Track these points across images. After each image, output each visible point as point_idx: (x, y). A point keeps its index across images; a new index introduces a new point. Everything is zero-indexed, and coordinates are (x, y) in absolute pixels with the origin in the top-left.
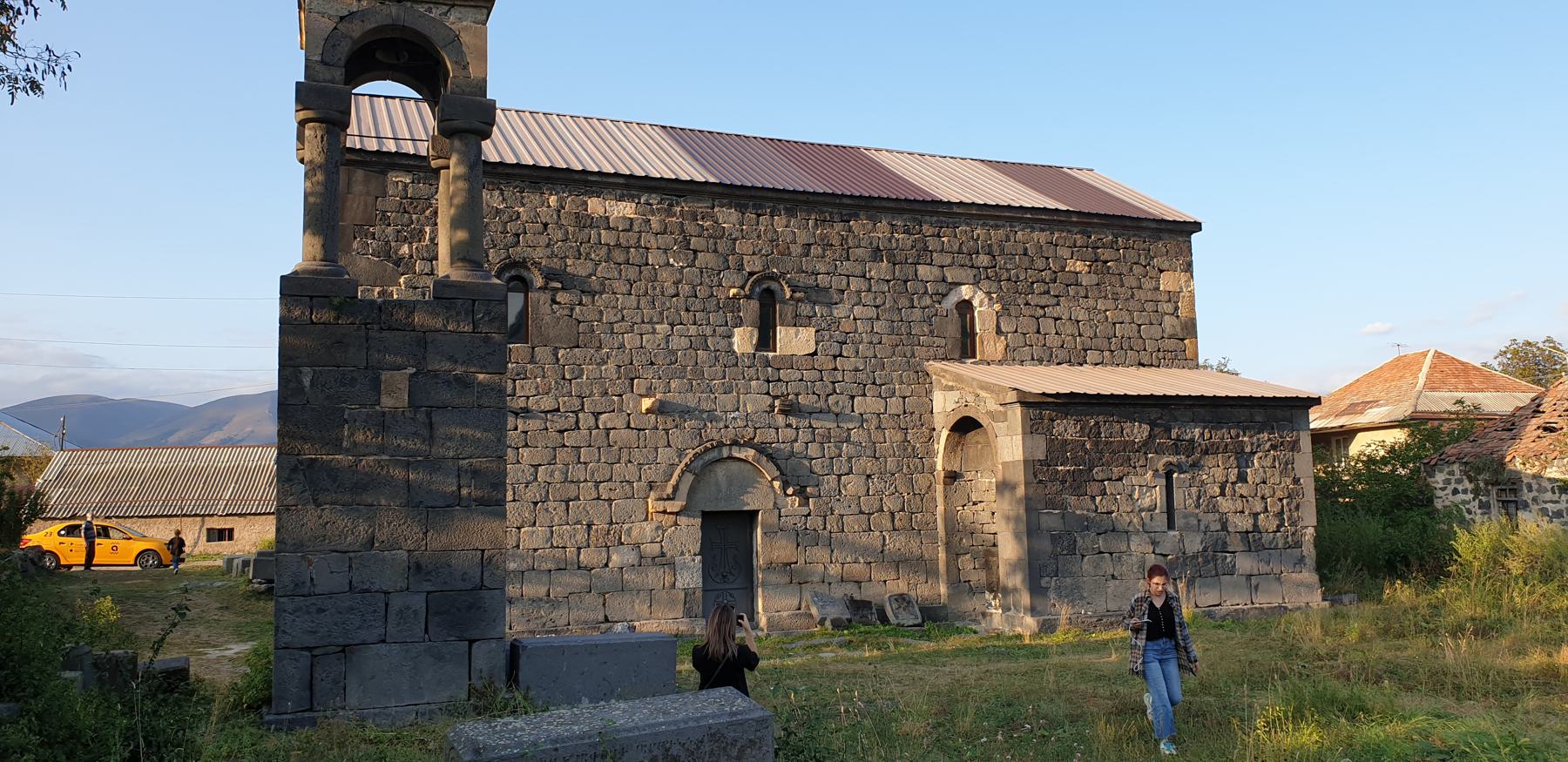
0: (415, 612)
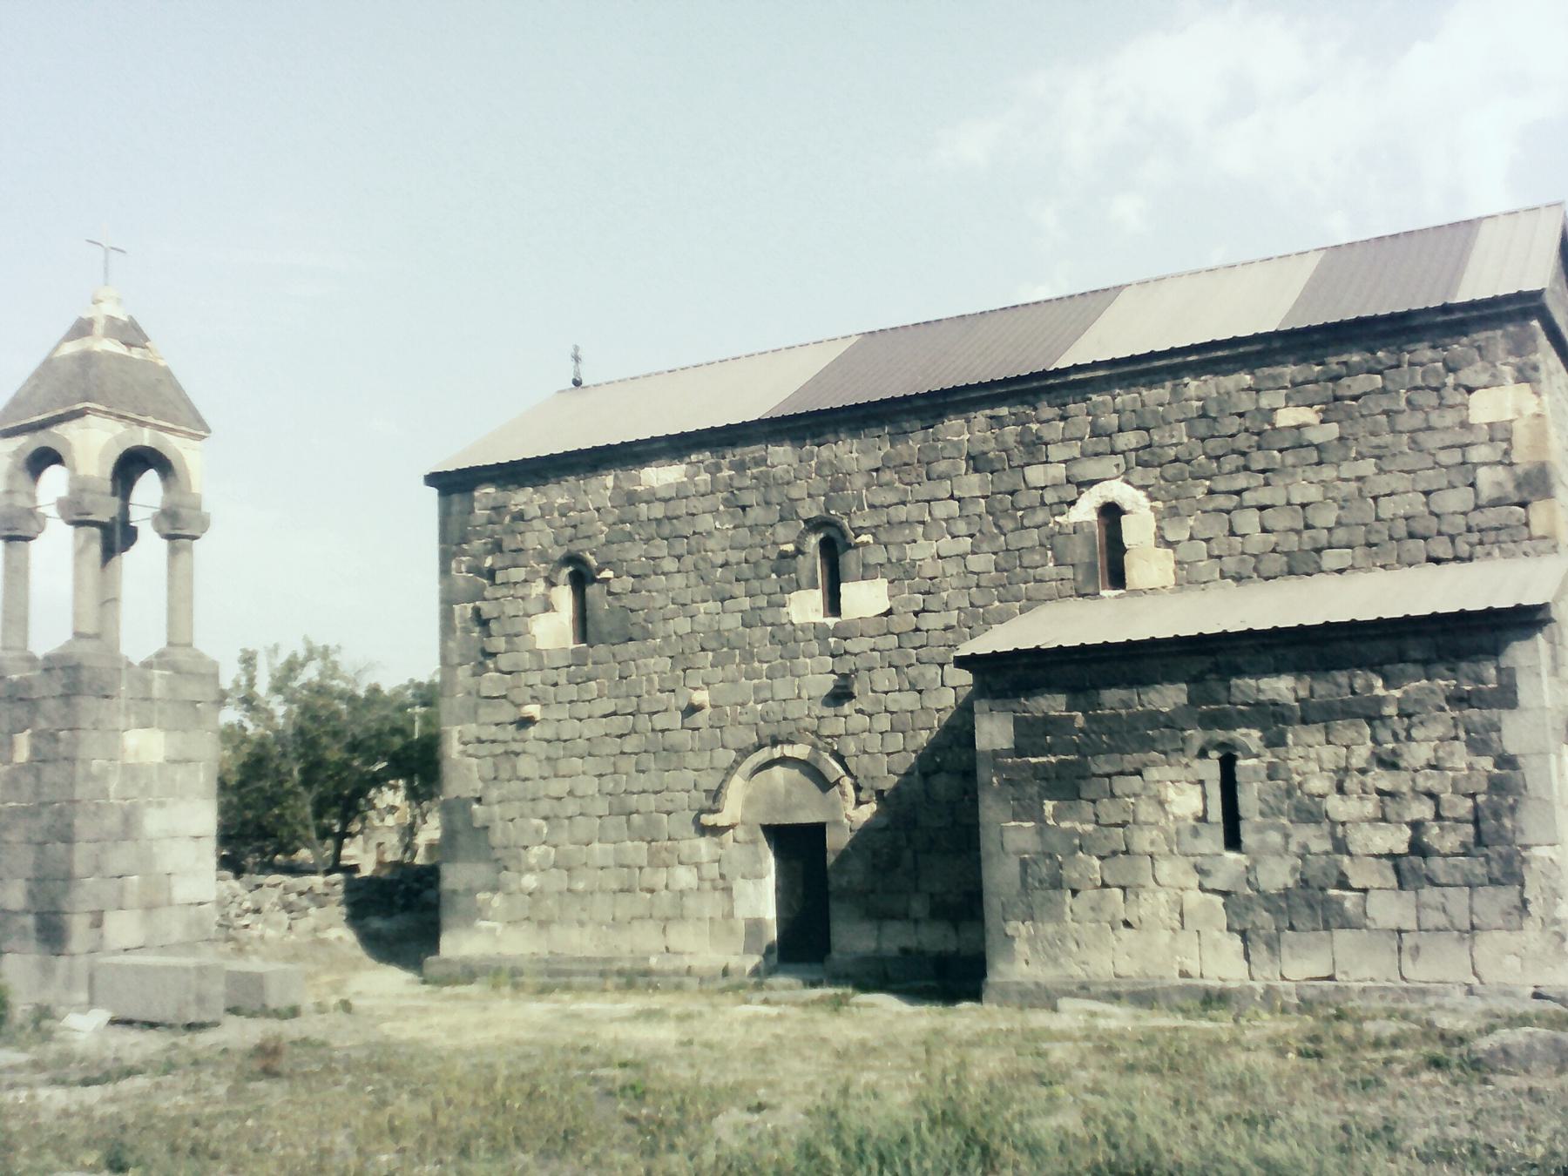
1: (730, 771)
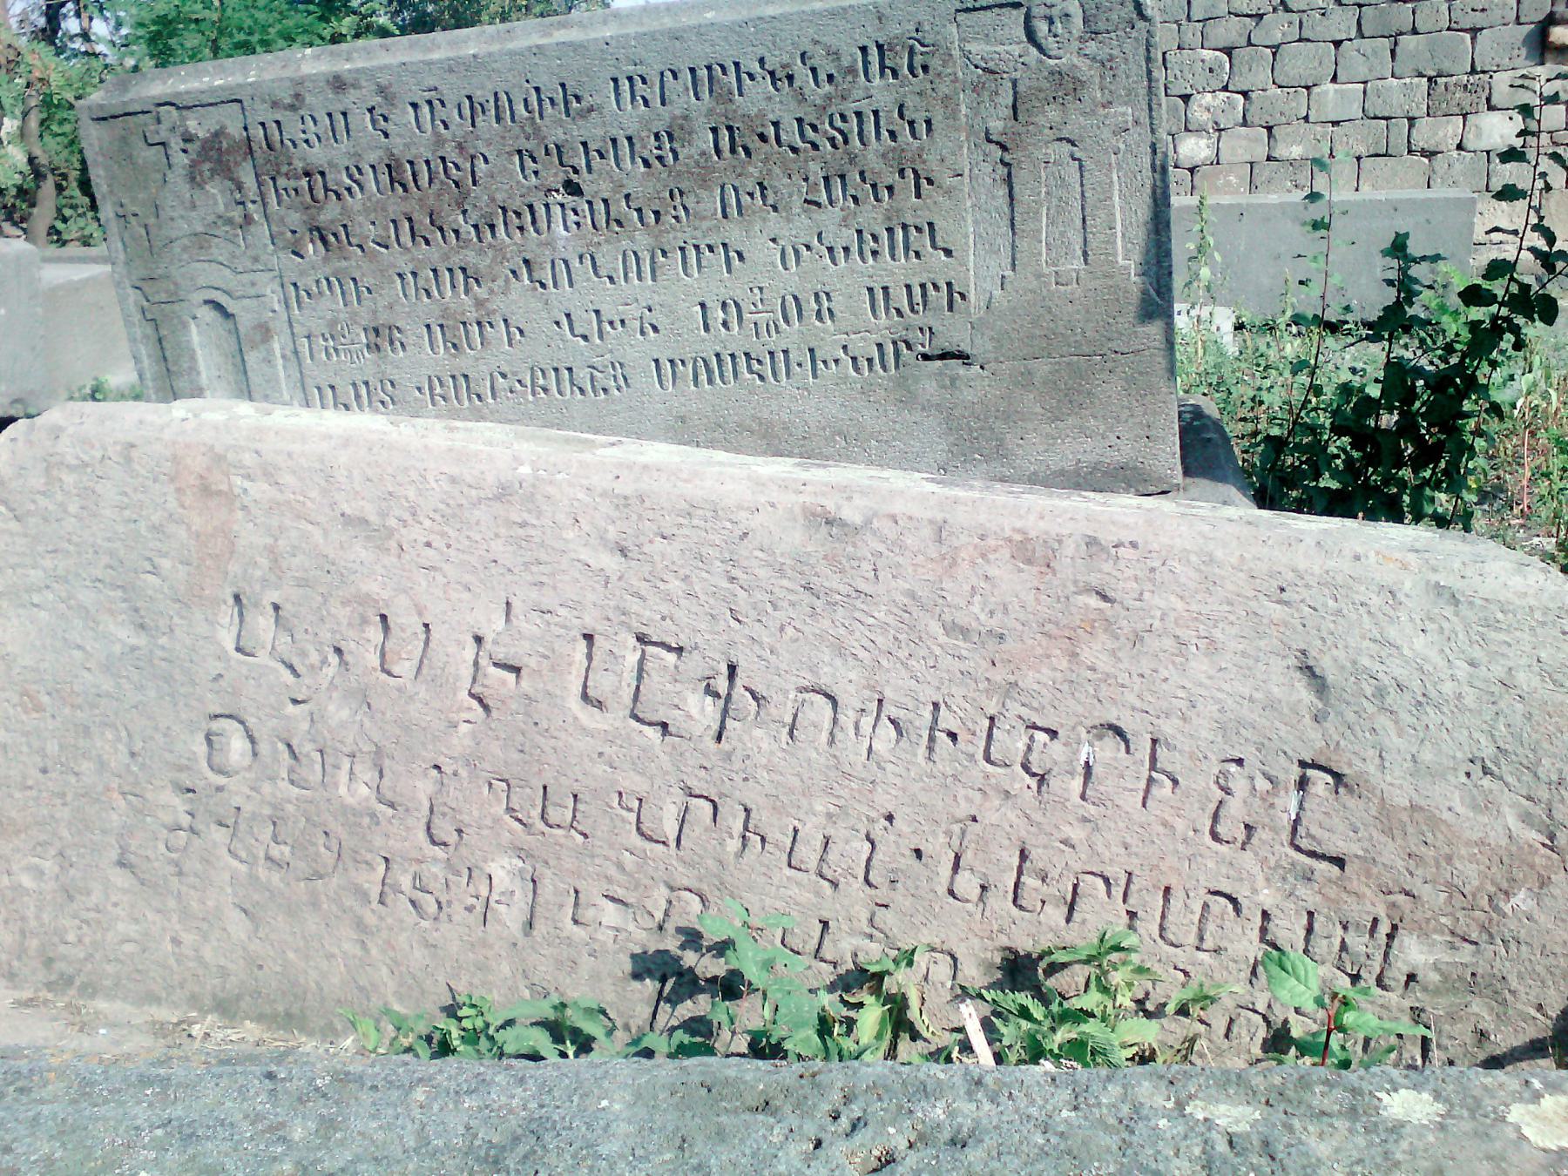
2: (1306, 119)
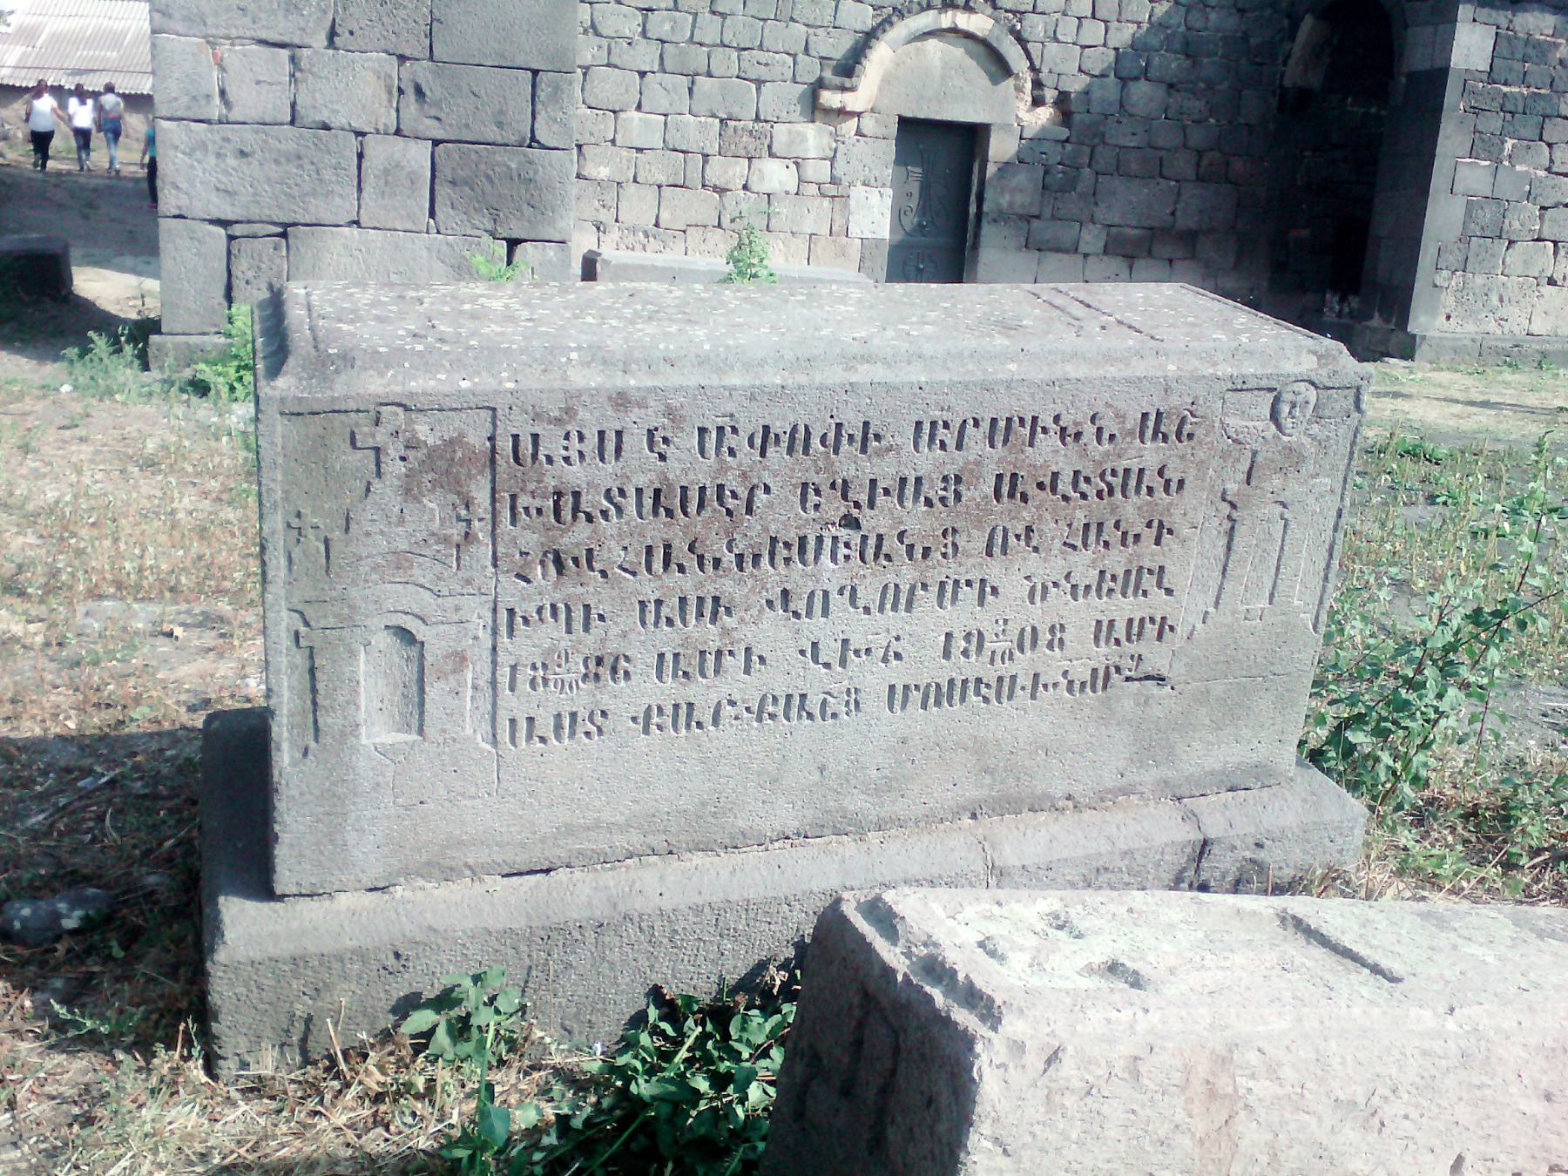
0: (413, 180)
1: (868, 39)
2: (613, 142)
